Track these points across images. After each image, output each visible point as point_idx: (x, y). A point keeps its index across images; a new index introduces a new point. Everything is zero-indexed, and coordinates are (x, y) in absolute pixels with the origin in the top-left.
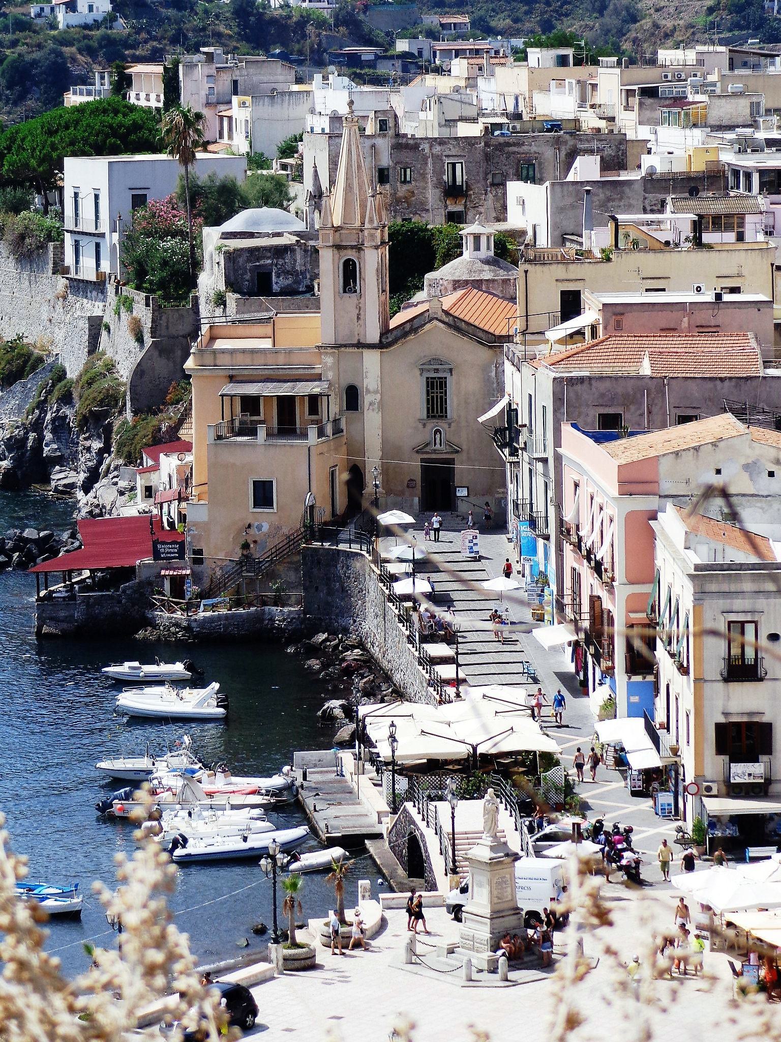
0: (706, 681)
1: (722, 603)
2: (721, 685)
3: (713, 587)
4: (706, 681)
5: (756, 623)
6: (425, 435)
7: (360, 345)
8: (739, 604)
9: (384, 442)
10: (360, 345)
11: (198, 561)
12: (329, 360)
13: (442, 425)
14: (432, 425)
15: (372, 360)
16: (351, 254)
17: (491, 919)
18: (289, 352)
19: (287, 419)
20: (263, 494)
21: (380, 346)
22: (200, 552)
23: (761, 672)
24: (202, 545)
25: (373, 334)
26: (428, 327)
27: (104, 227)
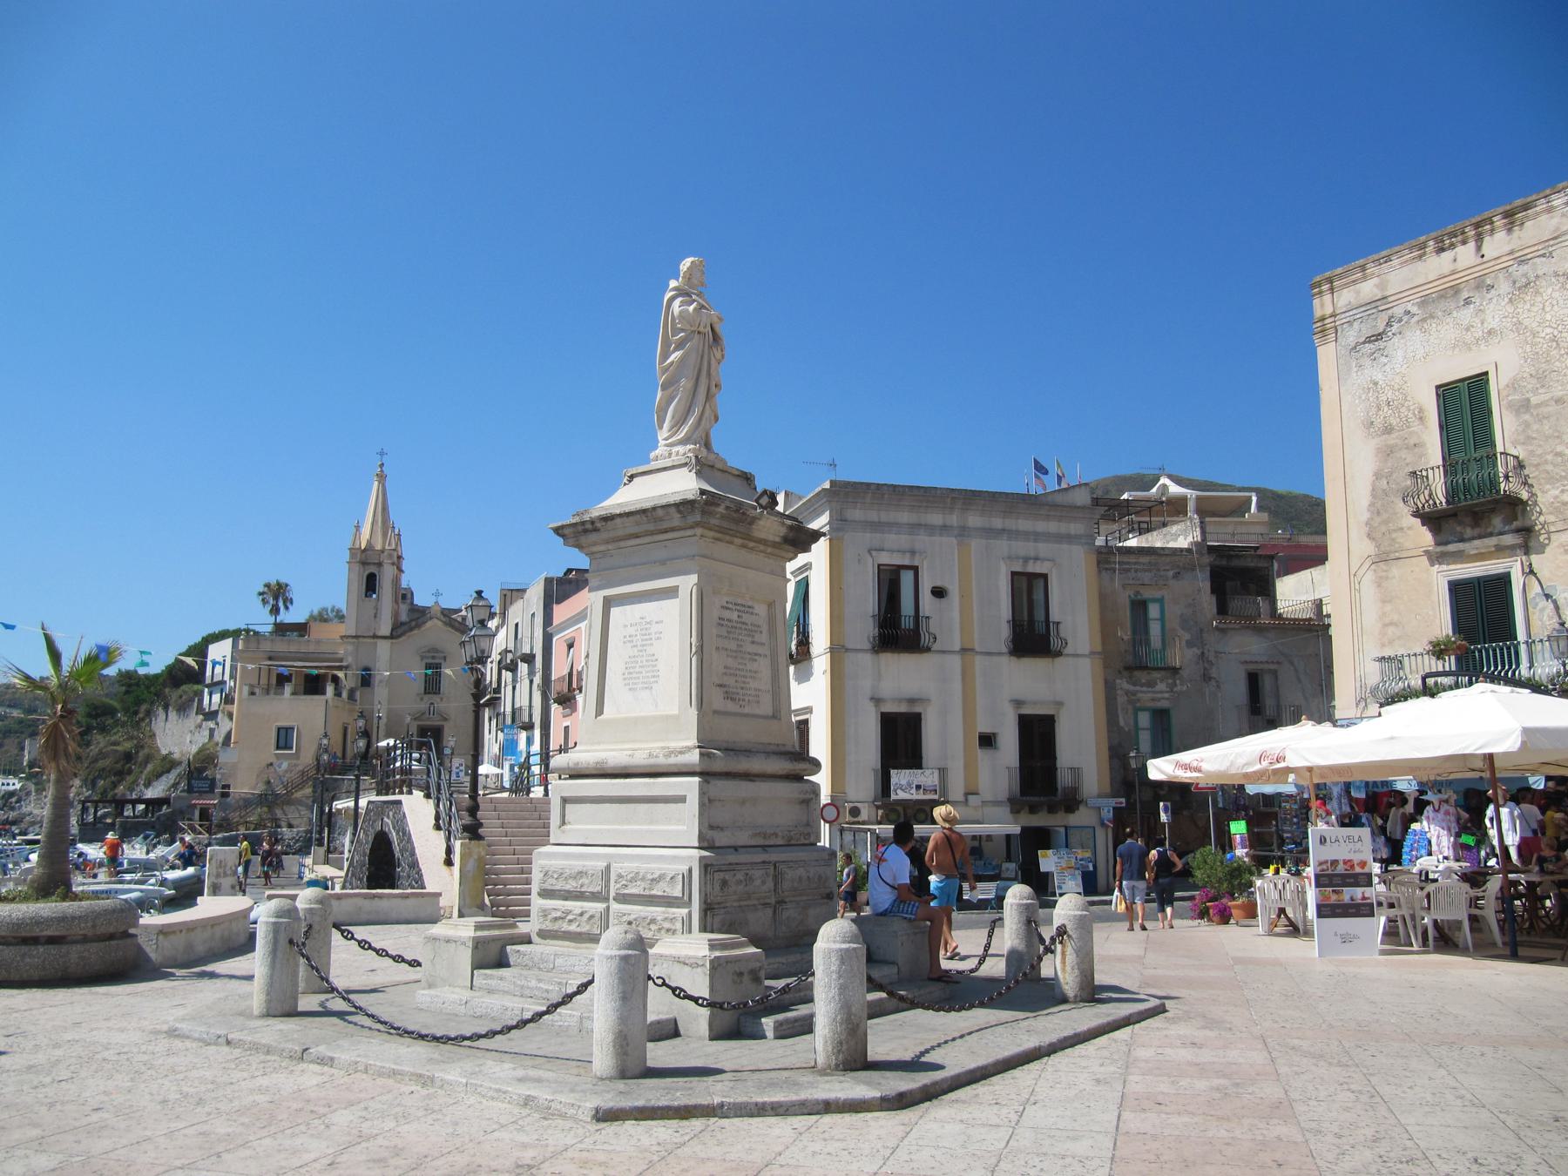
0: (847, 650)
1: (868, 538)
2: (868, 658)
3: (856, 514)
4: (847, 650)
5: (915, 569)
6: (423, 706)
7: (375, 637)
8: (891, 539)
9: (390, 712)
10: (375, 637)
11: (225, 795)
12: (350, 648)
13: (436, 698)
14: (426, 697)
15: (384, 648)
16: (373, 569)
17: (706, 775)
18: (318, 642)
19: (313, 685)
20: (284, 738)
21: (392, 637)
22: (228, 786)
23: (925, 639)
24: (230, 782)
25: (385, 629)
26: (429, 624)
27: (227, 677)
